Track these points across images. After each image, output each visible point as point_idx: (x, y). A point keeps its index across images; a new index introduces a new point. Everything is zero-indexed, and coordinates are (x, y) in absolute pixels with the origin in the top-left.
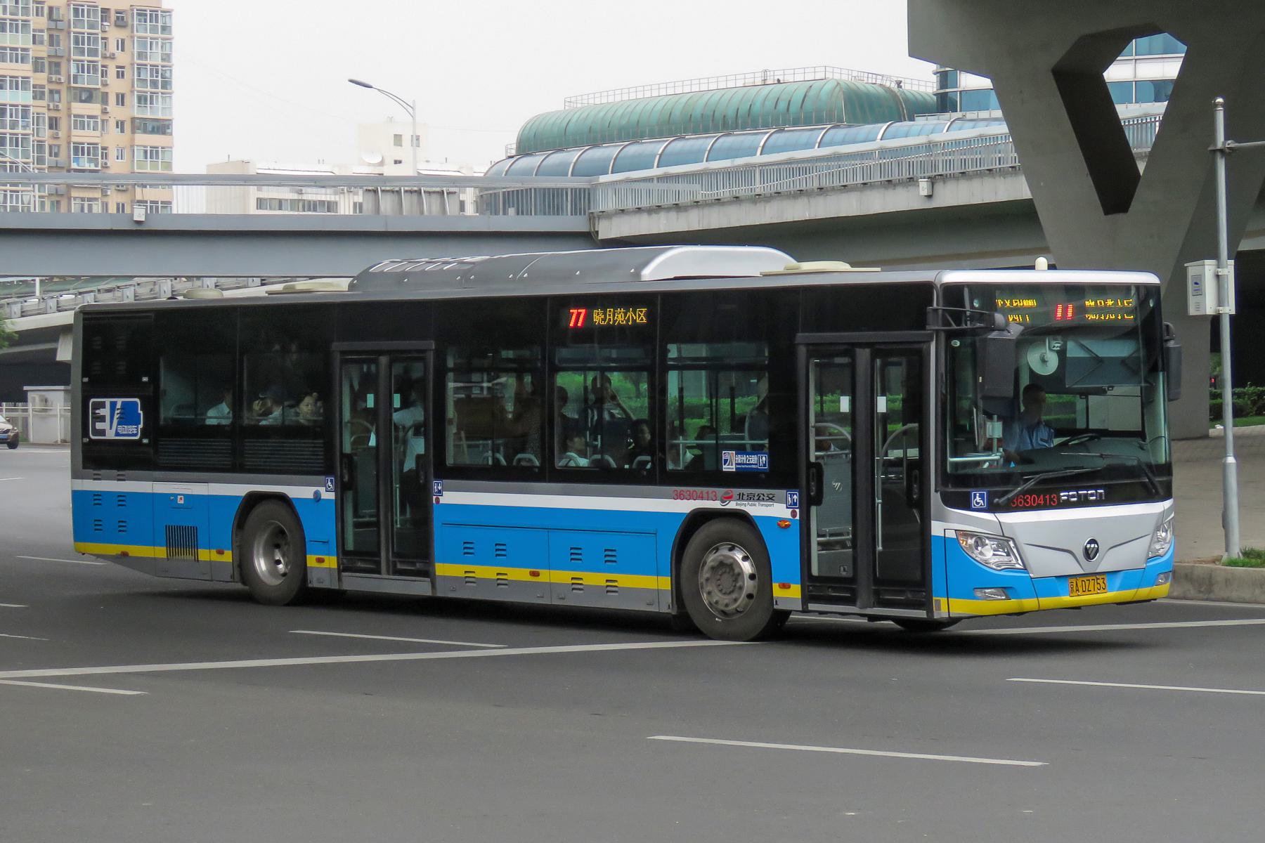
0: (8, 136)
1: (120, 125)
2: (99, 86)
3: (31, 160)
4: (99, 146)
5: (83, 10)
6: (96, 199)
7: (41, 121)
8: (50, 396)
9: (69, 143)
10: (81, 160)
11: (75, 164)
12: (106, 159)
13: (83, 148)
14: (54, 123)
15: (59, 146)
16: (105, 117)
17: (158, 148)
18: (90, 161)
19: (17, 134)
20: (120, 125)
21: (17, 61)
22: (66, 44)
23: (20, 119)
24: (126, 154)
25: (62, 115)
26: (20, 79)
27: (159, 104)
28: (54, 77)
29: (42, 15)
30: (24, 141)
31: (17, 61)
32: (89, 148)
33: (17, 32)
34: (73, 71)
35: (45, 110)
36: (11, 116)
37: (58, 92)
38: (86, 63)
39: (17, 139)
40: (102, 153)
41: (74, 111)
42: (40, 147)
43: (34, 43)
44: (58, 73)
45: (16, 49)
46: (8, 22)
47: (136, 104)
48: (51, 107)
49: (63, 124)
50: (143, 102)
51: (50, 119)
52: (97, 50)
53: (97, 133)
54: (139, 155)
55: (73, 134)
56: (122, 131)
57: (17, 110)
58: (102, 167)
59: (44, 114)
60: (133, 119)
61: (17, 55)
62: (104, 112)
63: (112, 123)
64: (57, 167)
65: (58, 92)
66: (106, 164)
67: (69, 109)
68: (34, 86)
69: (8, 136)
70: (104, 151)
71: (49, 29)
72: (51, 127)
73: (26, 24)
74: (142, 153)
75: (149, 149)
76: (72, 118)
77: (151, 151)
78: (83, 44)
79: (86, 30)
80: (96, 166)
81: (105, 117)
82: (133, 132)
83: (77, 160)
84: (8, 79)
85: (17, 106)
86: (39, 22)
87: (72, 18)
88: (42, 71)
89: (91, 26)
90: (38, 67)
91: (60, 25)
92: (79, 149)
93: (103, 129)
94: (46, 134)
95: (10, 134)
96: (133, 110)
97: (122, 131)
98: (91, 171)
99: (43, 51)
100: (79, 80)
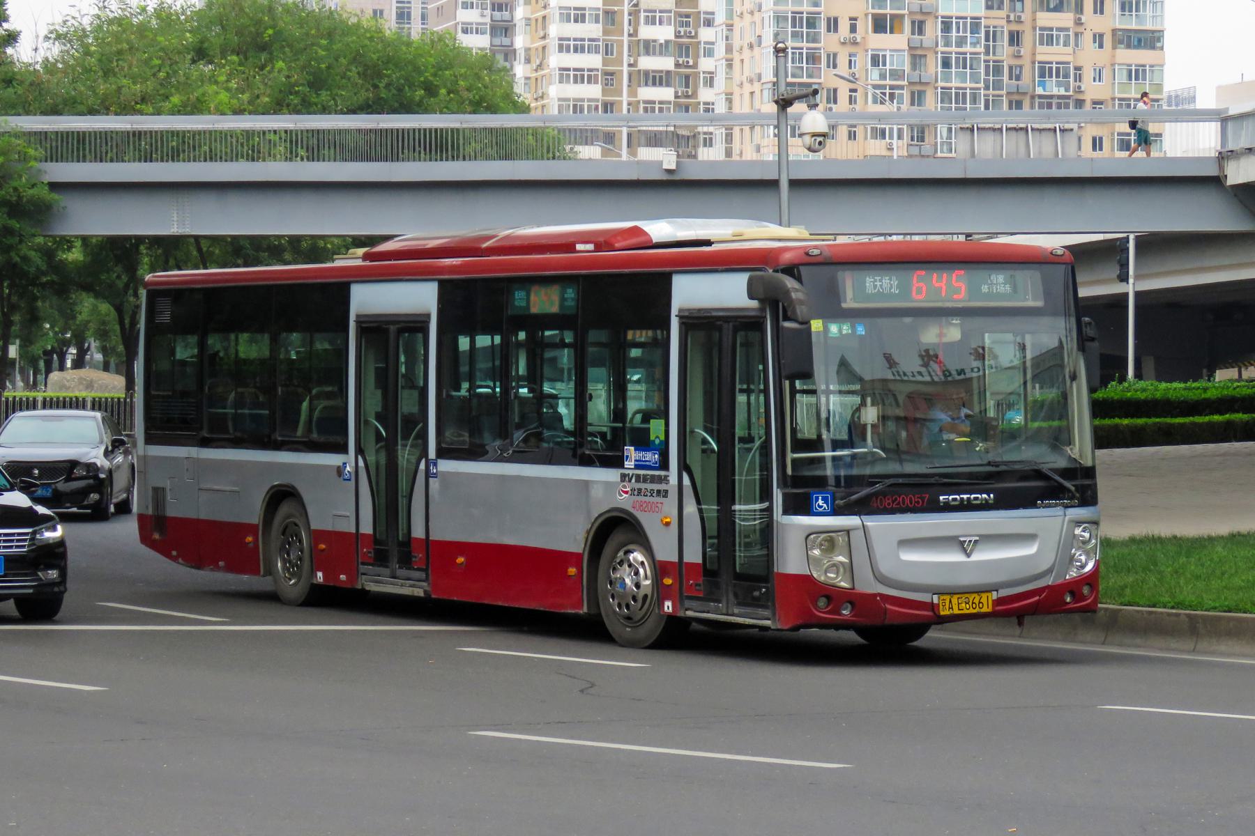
0: (954, 56)
1: (1099, 39)
3: (982, 85)
4: (1071, 66)
7: (998, 34)
9: (1033, 63)
10: (1048, 84)
11: (1041, 88)
12: (1080, 81)
13: (1051, 69)
14: (1015, 38)
15: (1021, 67)
16: (1080, 29)
17: (1144, 66)
18: (1059, 85)
19: (966, 54)
20: (1099, 39)
24: (1105, 74)
25: (1026, 29)
27: (1149, 13)
32: (1058, 69)
35: (1004, 22)
36: (958, 32)
39: (965, 59)
40: (1075, 74)
41: (1040, 23)
42: (998, 70)
47: (1118, 11)
48: (1012, 18)
49: (1027, 39)
50: (1127, 9)
53: (1069, 50)
54: (1121, 76)
55: (1038, 51)
56: (1101, 46)
57: (965, 24)
58: (1075, 91)
59: (1003, 27)
60: (1114, 31)
62: (1078, 23)
63: (1088, 37)
64: (1018, 92)
66: (1079, 87)
67: (1034, 20)
69: (954, 56)
70: (1078, 72)
74: (1125, 73)
75: (1133, 68)
76: (1038, 32)
77: (1137, 71)
80: (1067, 90)
81: (1080, 29)
82: (1114, 48)
83: (1042, 84)
85: (966, 18)
92: (1045, 71)
93: (1077, 45)
94: (1004, 51)
95: (956, 53)
96: (1113, 19)
97: (1101, 46)
98: (1060, 97)
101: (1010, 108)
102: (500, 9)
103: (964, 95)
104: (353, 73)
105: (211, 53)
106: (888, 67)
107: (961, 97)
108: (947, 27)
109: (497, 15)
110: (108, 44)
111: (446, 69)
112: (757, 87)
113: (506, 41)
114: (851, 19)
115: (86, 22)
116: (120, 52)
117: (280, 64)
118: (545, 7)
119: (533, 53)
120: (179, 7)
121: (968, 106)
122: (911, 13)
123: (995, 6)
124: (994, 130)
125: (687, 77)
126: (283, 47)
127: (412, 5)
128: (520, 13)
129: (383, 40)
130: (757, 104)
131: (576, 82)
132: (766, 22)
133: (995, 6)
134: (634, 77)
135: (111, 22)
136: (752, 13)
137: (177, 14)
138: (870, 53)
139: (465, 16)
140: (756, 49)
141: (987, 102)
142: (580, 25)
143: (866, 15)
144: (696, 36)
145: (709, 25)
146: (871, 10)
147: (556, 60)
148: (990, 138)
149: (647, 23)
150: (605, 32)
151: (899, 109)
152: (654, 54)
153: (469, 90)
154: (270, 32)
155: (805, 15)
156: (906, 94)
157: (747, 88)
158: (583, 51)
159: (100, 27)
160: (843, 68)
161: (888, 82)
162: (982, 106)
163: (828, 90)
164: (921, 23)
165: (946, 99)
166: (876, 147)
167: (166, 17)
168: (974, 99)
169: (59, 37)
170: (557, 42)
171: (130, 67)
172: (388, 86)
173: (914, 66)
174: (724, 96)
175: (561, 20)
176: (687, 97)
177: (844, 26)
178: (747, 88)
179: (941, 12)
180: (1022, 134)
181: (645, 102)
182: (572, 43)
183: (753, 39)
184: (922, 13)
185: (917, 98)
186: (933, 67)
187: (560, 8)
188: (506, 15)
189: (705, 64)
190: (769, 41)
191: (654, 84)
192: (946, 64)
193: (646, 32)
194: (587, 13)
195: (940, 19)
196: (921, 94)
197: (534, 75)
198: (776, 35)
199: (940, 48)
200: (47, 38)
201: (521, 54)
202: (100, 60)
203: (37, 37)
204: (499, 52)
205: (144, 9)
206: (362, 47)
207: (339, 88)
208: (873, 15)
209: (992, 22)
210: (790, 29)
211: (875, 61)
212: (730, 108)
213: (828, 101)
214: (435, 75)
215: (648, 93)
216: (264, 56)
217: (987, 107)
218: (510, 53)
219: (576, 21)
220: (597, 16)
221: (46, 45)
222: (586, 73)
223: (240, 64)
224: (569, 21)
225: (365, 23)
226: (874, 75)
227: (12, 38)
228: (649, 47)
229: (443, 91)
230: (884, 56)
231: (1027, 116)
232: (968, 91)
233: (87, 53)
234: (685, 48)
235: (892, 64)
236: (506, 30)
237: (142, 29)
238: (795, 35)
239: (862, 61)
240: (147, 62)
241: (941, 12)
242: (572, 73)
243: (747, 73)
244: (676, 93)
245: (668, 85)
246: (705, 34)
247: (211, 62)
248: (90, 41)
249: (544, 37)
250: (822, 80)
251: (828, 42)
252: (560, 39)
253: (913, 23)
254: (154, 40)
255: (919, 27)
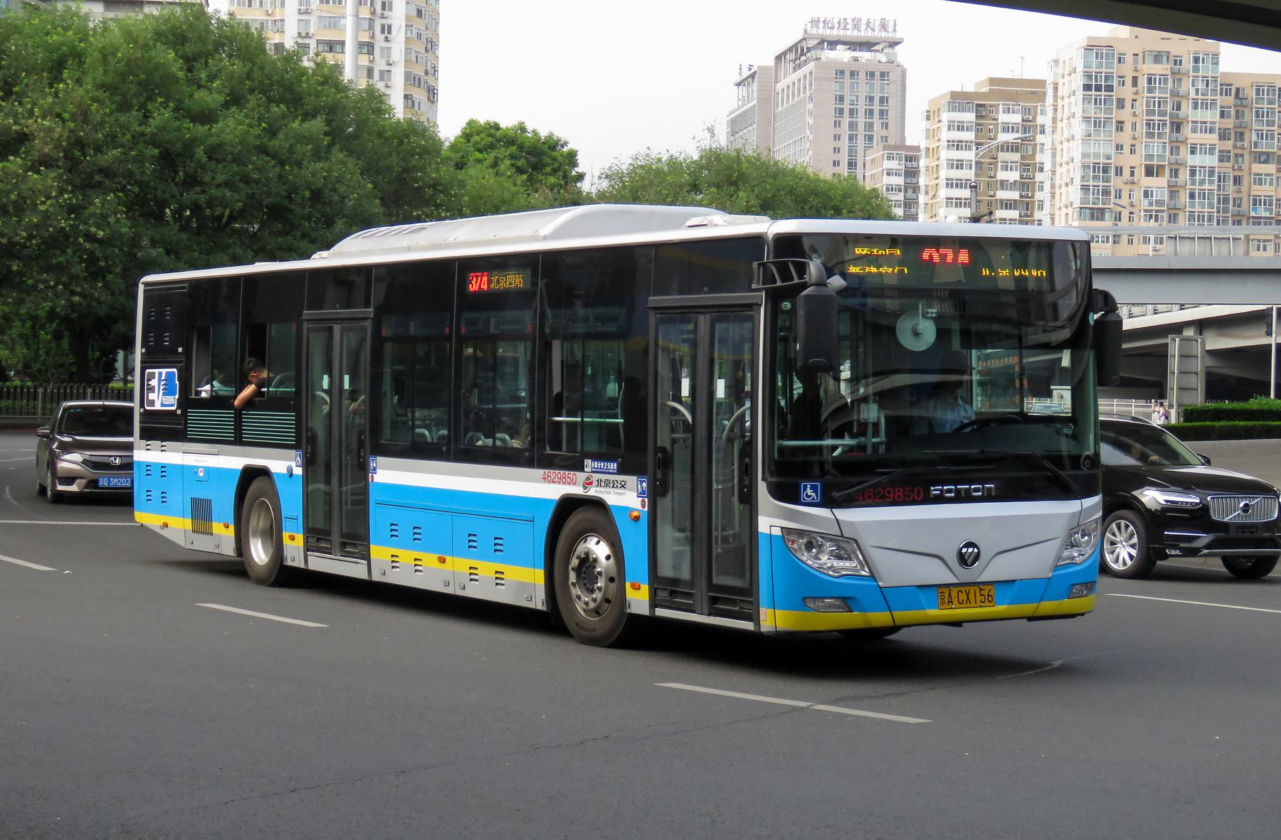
0: (1197, 191)
2: (1275, 150)
3: (1215, 210)
5: (1263, 90)
6: (1270, 241)
7: (1227, 178)
8: (1063, 392)
10: (1258, 210)
13: (1260, 200)
14: (1237, 180)
15: (1241, 199)
18: (1266, 210)
21: (1206, 132)
22: (1250, 117)
23: (1207, 178)
25: (1245, 174)
26: (1208, 146)
28: (1239, 144)
29: (1230, 95)
30: (1211, 196)
31: (1206, 132)
32: (1265, 200)
33: (1207, 109)
34: (1254, 138)
35: (1230, 170)
37: (1242, 156)
38: (1265, 132)
42: (1226, 200)
43: (1222, 115)
44: (1242, 140)
45: (1206, 123)
46: (1200, 101)
49: (1245, 181)
51: (1235, 178)
52: (1274, 121)
53: (1273, 188)
57: (1205, 171)
61: (1206, 127)
64: (1239, 215)
65: (1242, 156)
67: (1250, 169)
68: (1220, 151)
69: (1197, 191)
71: (1235, 106)
72: (1235, 183)
73: (1214, 102)
78: (1263, 117)
79: (1266, 106)
80: (1271, 214)
83: (1255, 210)
84: (1198, 146)
86: (1230, 100)
87: (1254, 96)
88: (1229, 139)
89: (1270, 102)
90: (1223, 136)
91: (1245, 102)
94: (1231, 189)
99: (1230, 123)
100: (1259, 145)
101: (1234, 225)
102: (911, 161)
103: (1204, 216)
104: (788, 200)
105: (701, 187)
106: (1154, 198)
107: (1201, 218)
108: (1193, 173)
109: (909, 164)
110: (637, 181)
111: (849, 198)
112: (1070, 210)
113: (914, 181)
114: (1131, 168)
115: (624, 168)
116: (644, 186)
117: (741, 194)
118: (938, 159)
119: (930, 188)
120: (682, 159)
121: (1206, 223)
122: (1170, 164)
123: (1225, 159)
124: (1190, 238)
125: (1027, 204)
126: (744, 183)
127: (858, 158)
128: (923, 163)
129: (808, 178)
130: (1070, 222)
131: (956, 206)
132: (1077, 169)
133: (1225, 159)
134: (994, 204)
135: (642, 167)
136: (1068, 163)
137: (681, 163)
138: (1143, 189)
139: (888, 164)
140: (1070, 186)
141: (1218, 221)
142: (959, 171)
143: (1141, 165)
144: (1033, 178)
145: (1042, 171)
146: (1144, 162)
147: (944, 193)
148: (1187, 242)
149: (1002, 170)
150: (976, 175)
151: (1160, 225)
152: (1007, 189)
153: (862, 210)
154: (735, 175)
155: (1101, 165)
156: (1165, 215)
157: (1064, 211)
158: (961, 187)
159: (634, 171)
160: (1124, 200)
161: (1154, 208)
162: (1215, 223)
163: (1116, 213)
164: (1177, 171)
165: (1192, 219)
166: (1149, 249)
167: (674, 164)
168: (1210, 219)
169: (607, 177)
170: (945, 182)
171: (649, 195)
172: (811, 208)
173: (1171, 198)
174: (1049, 216)
175: (948, 168)
176: (1028, 216)
177: (1126, 172)
178: (1064, 211)
179: (1189, 163)
180: (1208, 241)
181: (1001, 219)
182: (955, 182)
183: (1068, 181)
184: (1177, 163)
185: (1173, 218)
186: (1184, 198)
187: (947, 160)
188: (914, 164)
189: (1038, 196)
190: (1078, 182)
191: (1006, 208)
192: (1192, 196)
193: (1001, 175)
194: (964, 163)
195: (1188, 168)
196: (1175, 215)
197: (930, 202)
198: (1083, 177)
199: (1188, 186)
200: (600, 178)
201: (923, 189)
202: (631, 191)
203: (593, 176)
204: (910, 187)
205: (660, 160)
206: (796, 183)
207: (779, 209)
208: (1146, 165)
209: (1221, 170)
210: (1092, 174)
211: (1146, 194)
212: (1053, 224)
213: (1116, 220)
214: (841, 201)
215: (1000, 214)
216: (732, 189)
217: (1218, 224)
218: (916, 189)
219: (957, 168)
220: (971, 165)
221: (600, 182)
222: (963, 201)
223: (718, 194)
224: (952, 168)
225: (799, 169)
226: (1145, 204)
227: (581, 177)
228: (1004, 185)
229: (844, 211)
230: (1152, 191)
231: (1241, 231)
232: (1206, 214)
233: (624, 187)
234: (1026, 185)
235: (1157, 197)
236: (915, 173)
237: (658, 172)
238: (1094, 177)
239: (1137, 194)
240: (659, 193)
241: (1189, 163)
242: (954, 201)
243: (1063, 202)
244: (1020, 213)
245: (1015, 209)
246: (1039, 177)
247: (701, 193)
248: (627, 179)
249: (937, 178)
250: (1112, 206)
251: (1115, 182)
252: (947, 179)
253: (1171, 170)
254: (665, 179)
255: (1175, 173)
